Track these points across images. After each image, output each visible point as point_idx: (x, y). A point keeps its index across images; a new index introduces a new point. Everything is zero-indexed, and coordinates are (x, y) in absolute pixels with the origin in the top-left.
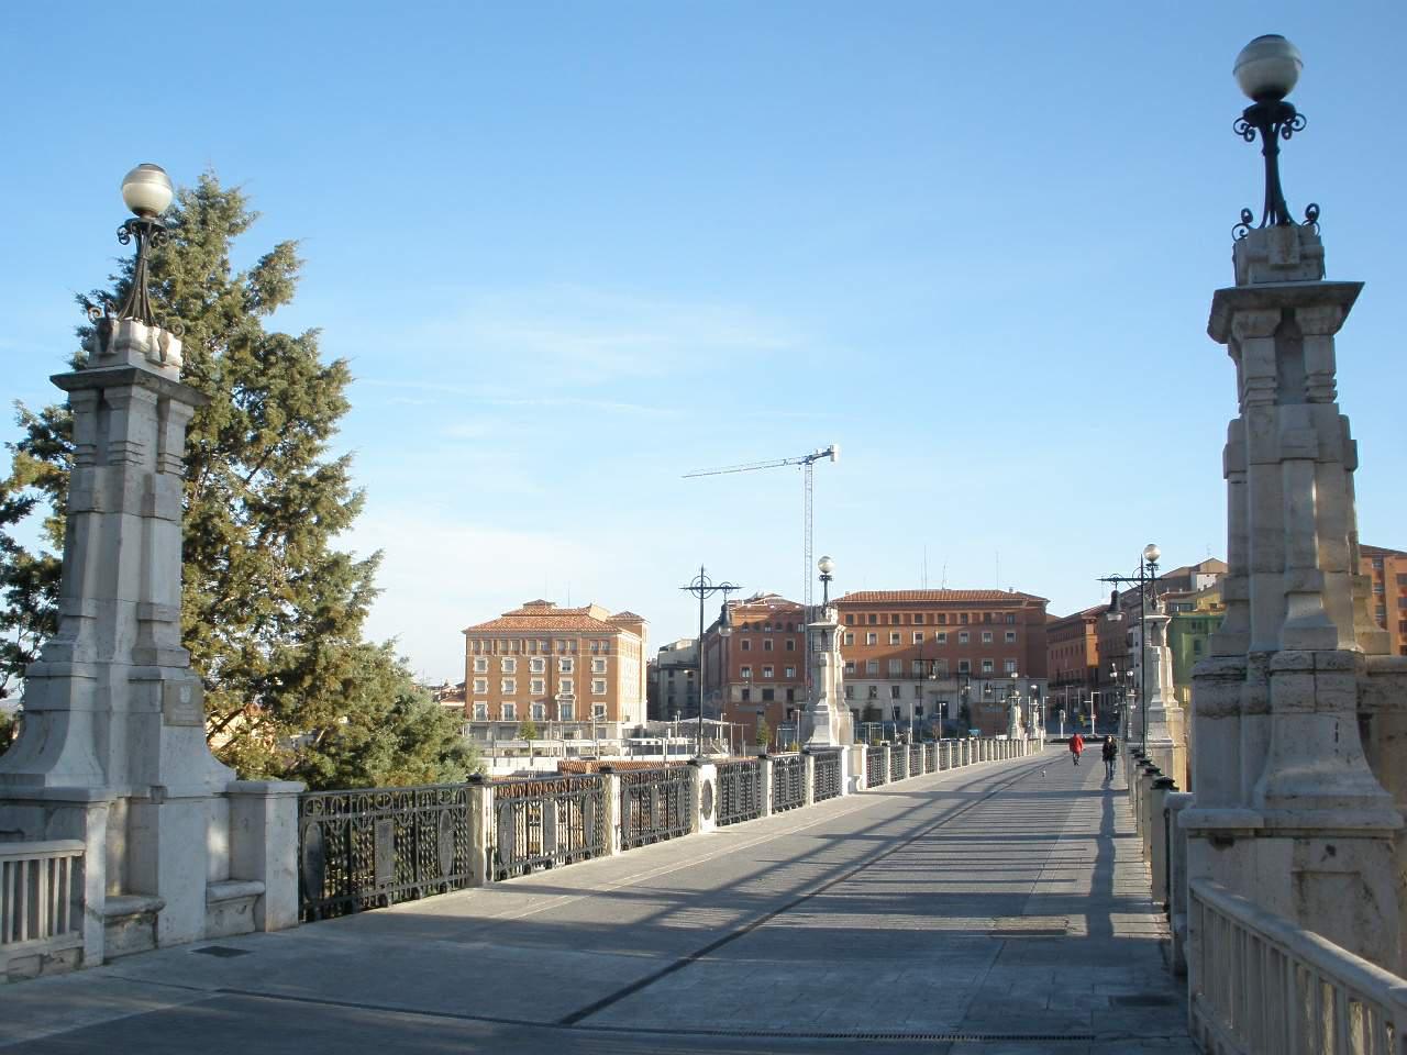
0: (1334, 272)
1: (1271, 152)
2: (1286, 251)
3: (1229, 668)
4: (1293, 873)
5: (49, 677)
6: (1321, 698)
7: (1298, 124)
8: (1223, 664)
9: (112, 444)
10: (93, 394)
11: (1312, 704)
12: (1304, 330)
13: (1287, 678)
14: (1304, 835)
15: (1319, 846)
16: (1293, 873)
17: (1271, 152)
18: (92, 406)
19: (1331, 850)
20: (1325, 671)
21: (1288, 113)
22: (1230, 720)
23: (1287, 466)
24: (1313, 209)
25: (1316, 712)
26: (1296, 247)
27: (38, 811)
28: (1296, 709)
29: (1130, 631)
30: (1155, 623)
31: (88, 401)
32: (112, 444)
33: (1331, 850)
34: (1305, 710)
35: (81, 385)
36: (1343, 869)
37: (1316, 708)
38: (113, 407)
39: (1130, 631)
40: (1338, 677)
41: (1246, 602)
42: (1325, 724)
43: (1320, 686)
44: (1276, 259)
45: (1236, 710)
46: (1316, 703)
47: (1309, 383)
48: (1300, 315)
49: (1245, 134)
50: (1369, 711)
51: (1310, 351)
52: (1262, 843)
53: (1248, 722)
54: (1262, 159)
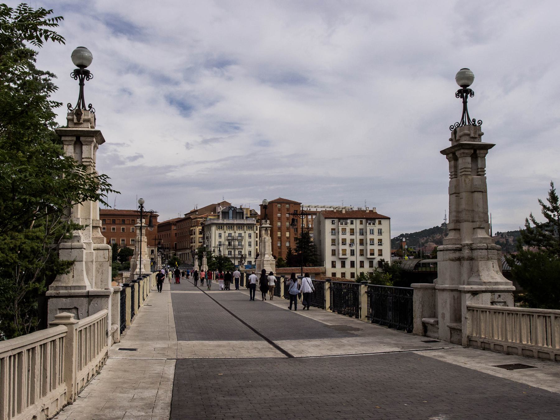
0: (484, 140)
1: (465, 103)
2: (475, 133)
3: (457, 247)
4: (491, 302)
5: (71, 249)
6: (489, 257)
8: (456, 247)
9: (83, 158)
10: (74, 138)
11: (487, 258)
12: (478, 155)
13: (481, 251)
14: (493, 292)
15: (497, 295)
16: (491, 302)
17: (465, 103)
18: (73, 142)
19: (499, 296)
20: (490, 249)
21: (472, 93)
22: (458, 262)
23: (476, 194)
25: (488, 260)
26: (478, 133)
27: (85, 300)
28: (483, 259)
29: (191, 229)
30: (266, 228)
31: (72, 140)
32: (83, 158)
34: (485, 259)
35: (70, 134)
36: (502, 301)
37: (488, 259)
38: (83, 144)
39: (191, 229)
40: (493, 251)
41: (459, 230)
42: (490, 263)
43: (489, 253)
44: (472, 135)
45: (459, 259)
46: (488, 258)
47: (479, 170)
48: (478, 152)
51: (479, 161)
52: (484, 294)
53: (466, 264)
54: (463, 104)
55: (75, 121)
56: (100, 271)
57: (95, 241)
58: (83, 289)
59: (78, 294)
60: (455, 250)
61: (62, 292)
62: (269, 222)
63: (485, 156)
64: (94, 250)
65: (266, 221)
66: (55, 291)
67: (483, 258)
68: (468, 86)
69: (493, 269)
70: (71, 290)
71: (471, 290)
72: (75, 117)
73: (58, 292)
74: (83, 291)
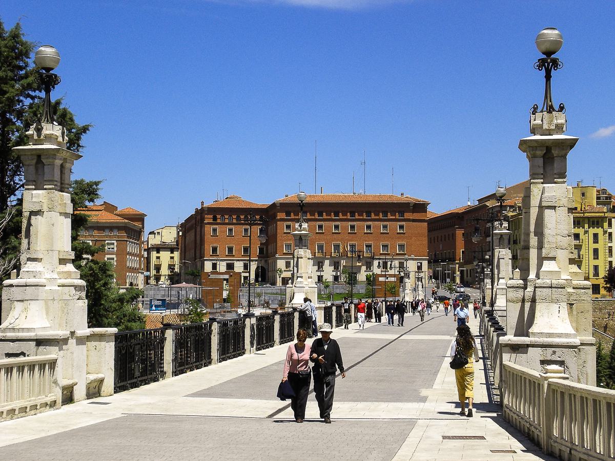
1: (548, 77)
2: (550, 123)
5: (26, 286)
6: (554, 298)
7: (560, 66)
17: (548, 77)
19: (554, 352)
20: (554, 288)
21: (555, 63)
24: (562, 105)
33: (554, 352)
42: (555, 307)
43: (554, 293)
44: (545, 126)
49: (539, 69)
50: (573, 302)
55: (36, 137)
56: (65, 310)
57: (61, 276)
58: (31, 332)
59: (26, 337)
60: (517, 287)
61: (10, 335)
62: (507, 225)
63: (566, 155)
64: (58, 286)
65: (501, 225)
66: (3, 334)
67: (544, 299)
68: (554, 53)
69: (559, 315)
70: (19, 332)
71: (509, 342)
72: (35, 133)
73: (4, 334)
74: (31, 335)
